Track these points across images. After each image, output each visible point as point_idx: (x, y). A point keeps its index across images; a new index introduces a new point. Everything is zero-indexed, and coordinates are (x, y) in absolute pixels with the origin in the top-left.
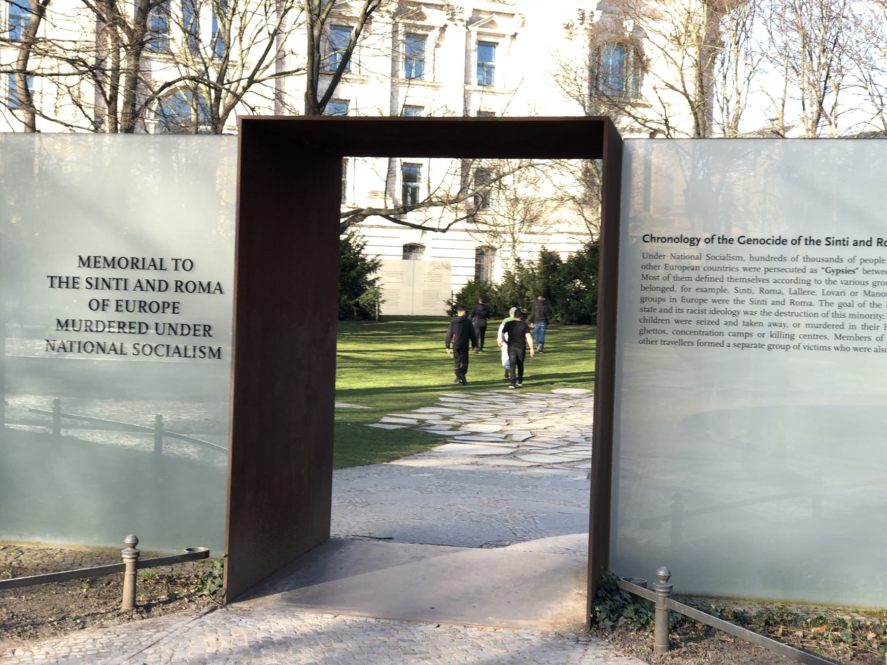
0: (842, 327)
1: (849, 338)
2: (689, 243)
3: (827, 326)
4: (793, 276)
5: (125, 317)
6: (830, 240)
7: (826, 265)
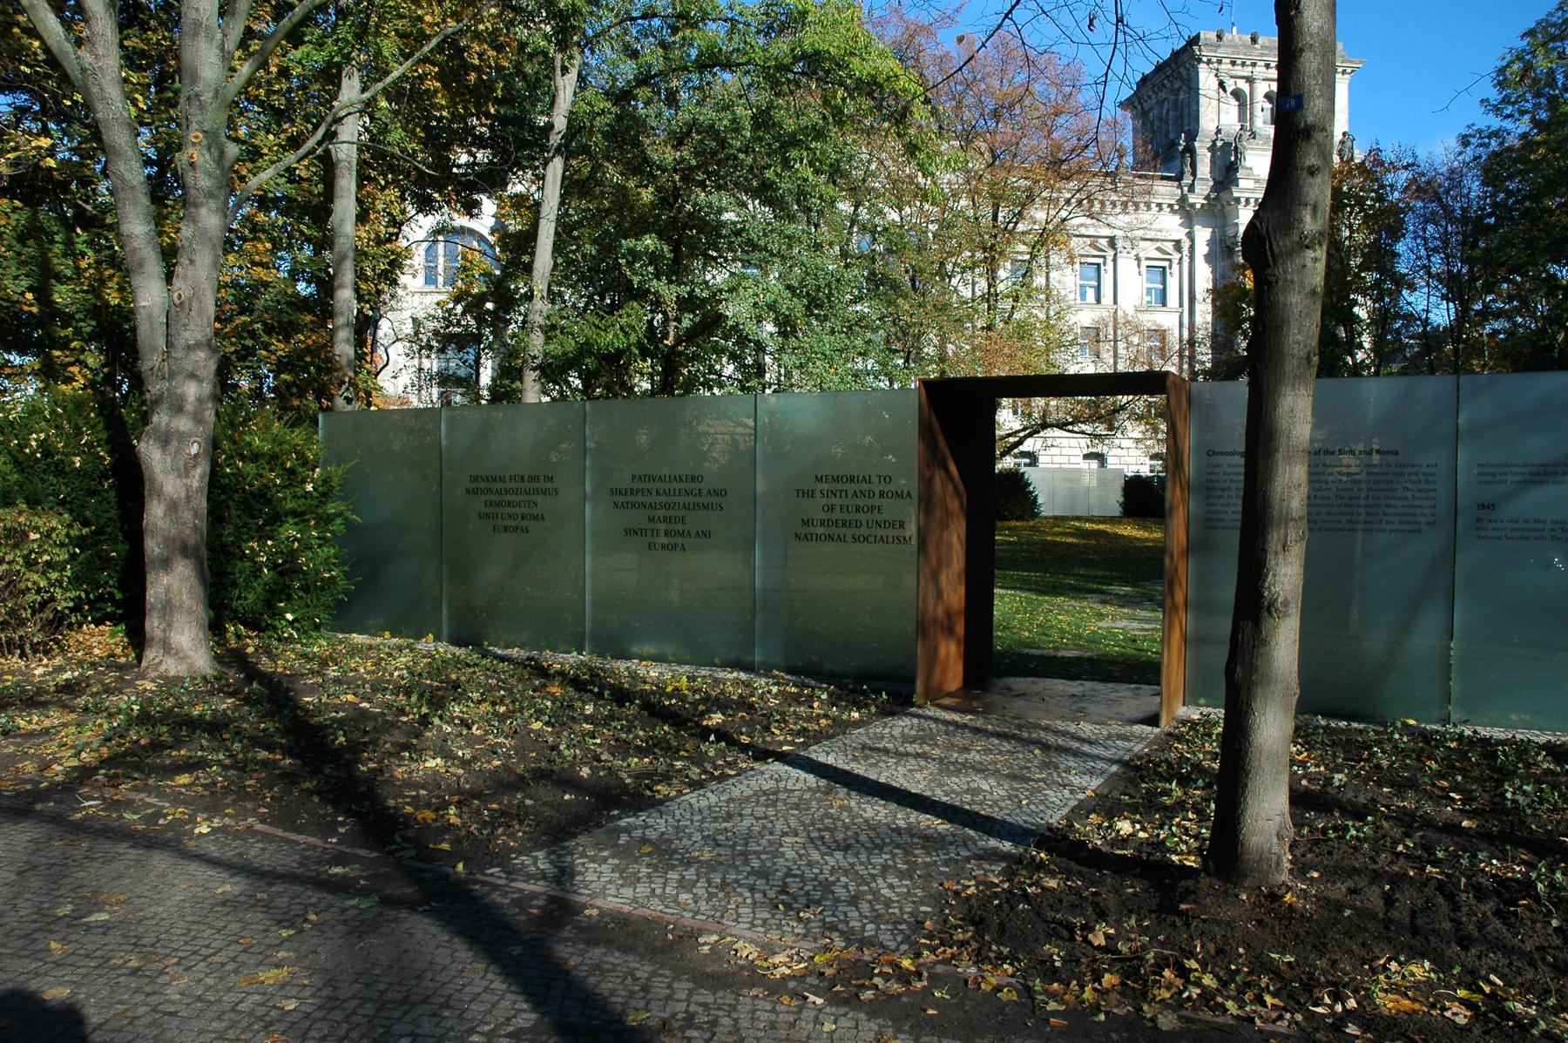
3: (1341, 514)
5: (847, 516)
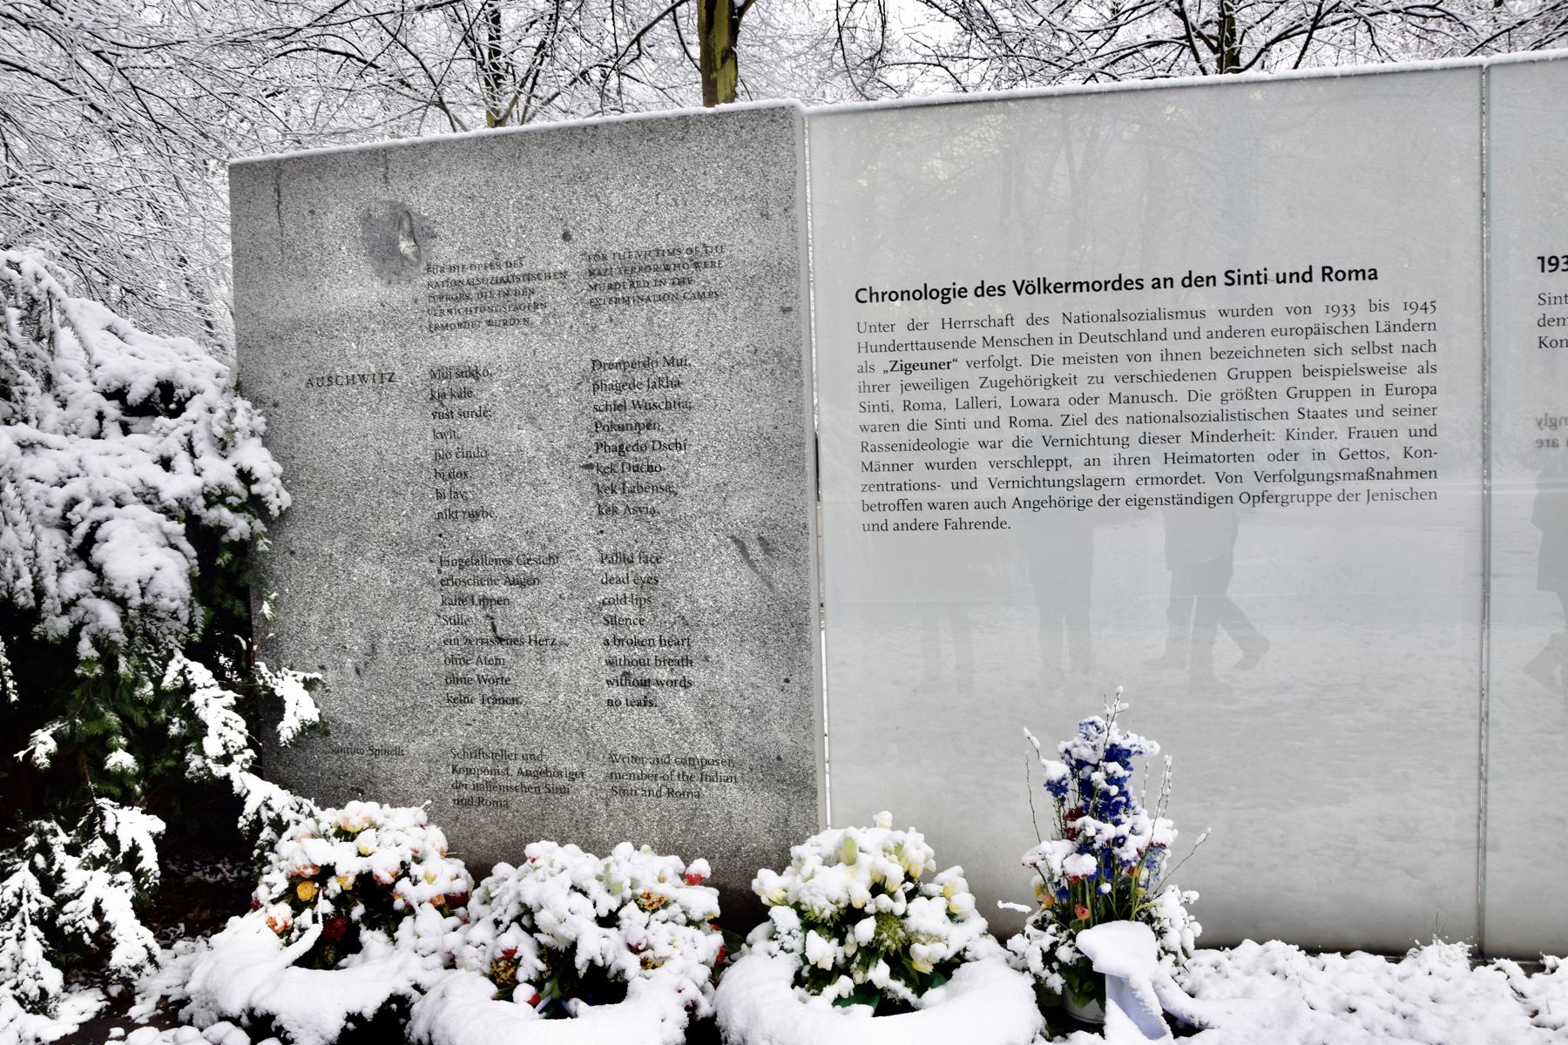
2: (940, 299)
6: (1234, 276)
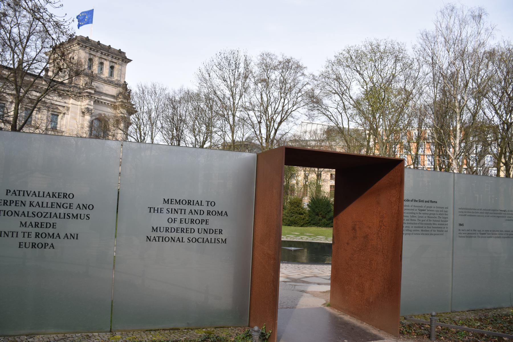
0: (422, 227)
1: (425, 231)
3: (419, 227)
4: (411, 211)
5: (184, 226)
7: (419, 208)
